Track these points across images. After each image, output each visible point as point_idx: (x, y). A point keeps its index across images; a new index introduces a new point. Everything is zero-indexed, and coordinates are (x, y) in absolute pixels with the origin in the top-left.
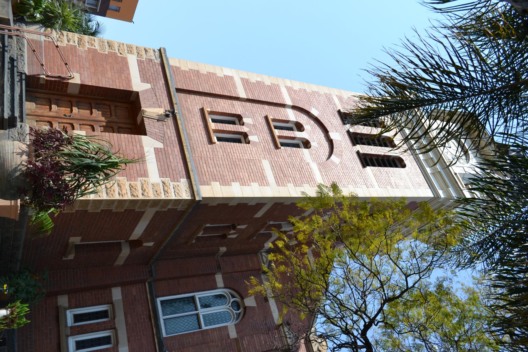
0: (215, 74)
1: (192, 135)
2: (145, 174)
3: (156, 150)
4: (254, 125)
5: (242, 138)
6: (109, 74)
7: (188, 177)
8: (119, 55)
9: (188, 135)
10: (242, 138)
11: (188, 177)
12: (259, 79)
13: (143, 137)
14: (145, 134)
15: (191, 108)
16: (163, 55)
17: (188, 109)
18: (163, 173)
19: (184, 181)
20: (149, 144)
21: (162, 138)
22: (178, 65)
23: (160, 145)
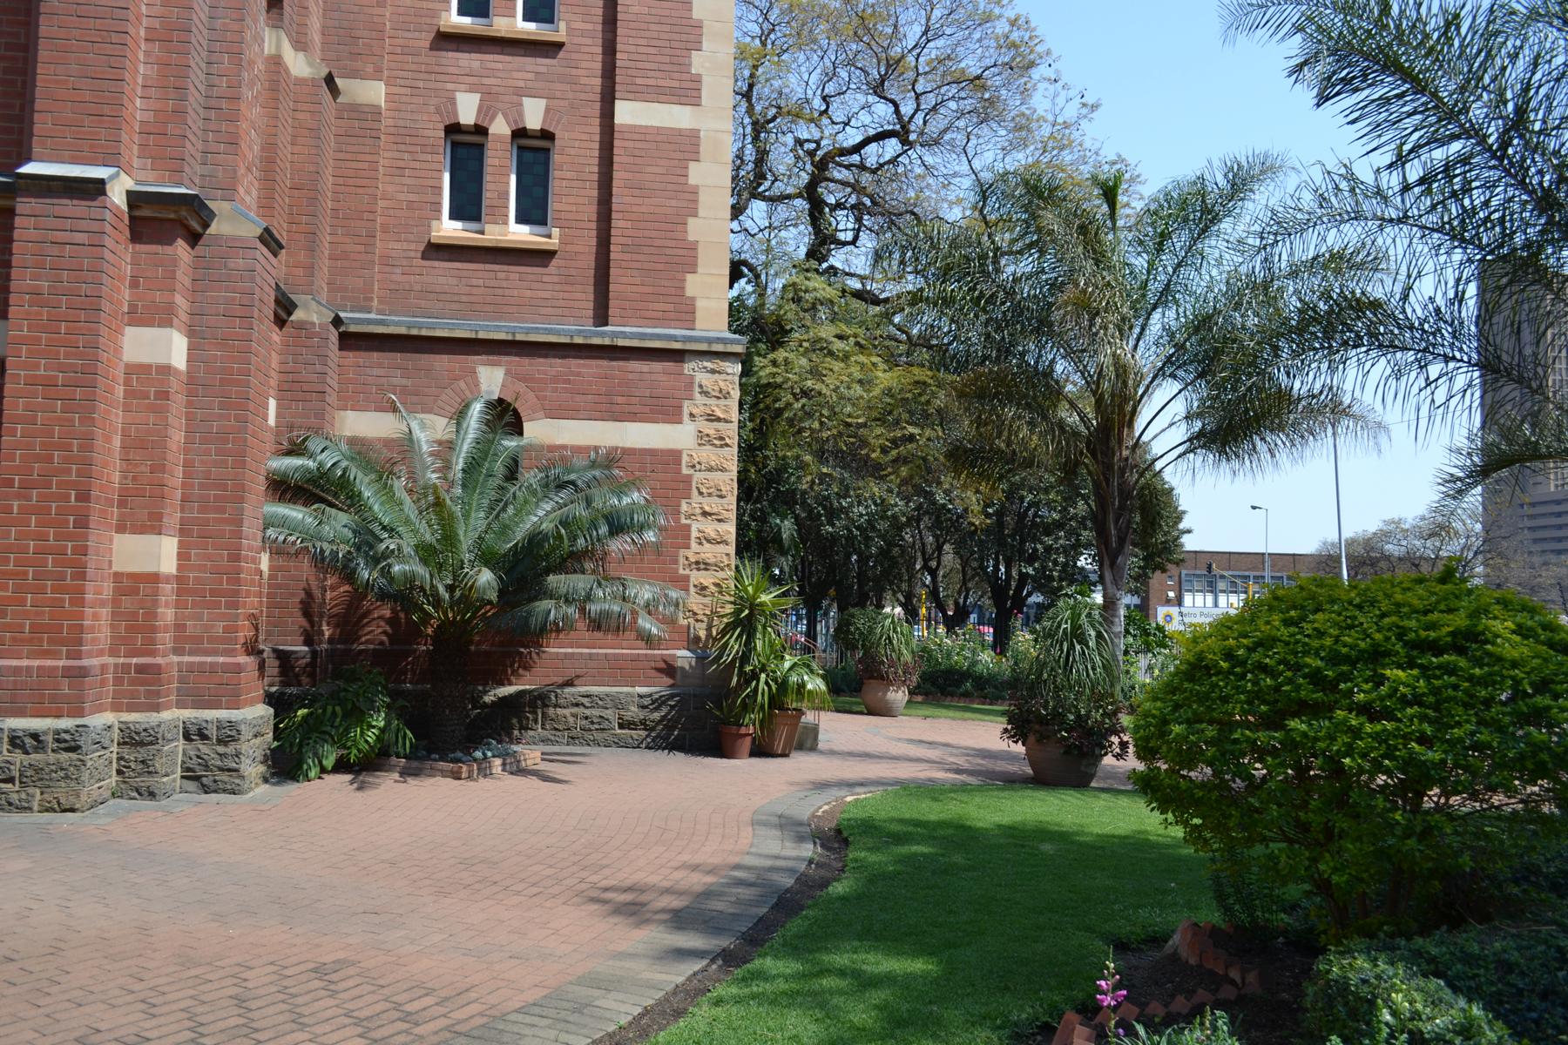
2: (674, 456)
5: (534, 150)
7: (678, 356)
10: (534, 150)
11: (678, 356)
18: (671, 414)
19: (689, 367)
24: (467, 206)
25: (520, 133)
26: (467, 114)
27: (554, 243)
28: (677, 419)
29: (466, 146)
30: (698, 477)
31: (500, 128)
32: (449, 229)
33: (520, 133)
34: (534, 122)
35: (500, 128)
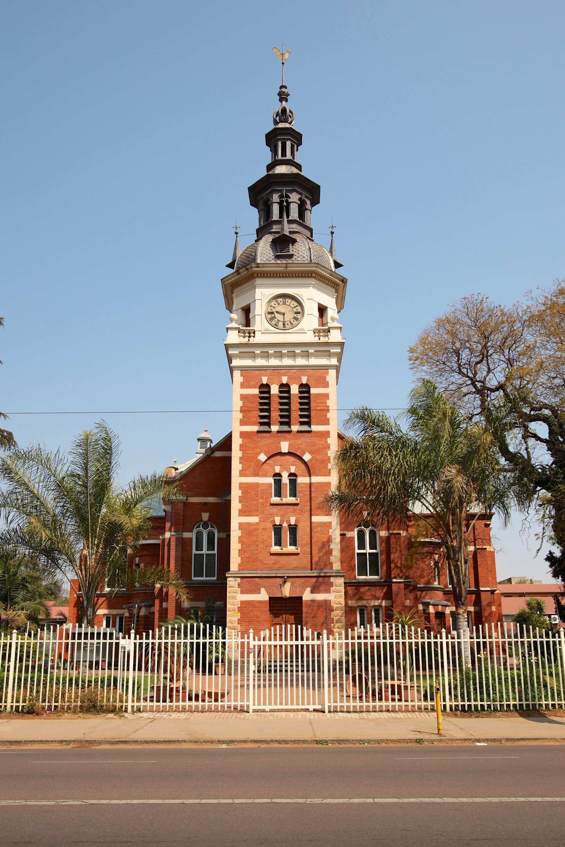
0: (240, 537)
1: (295, 566)
3: (312, 592)
4: (281, 516)
5: (293, 529)
6: (259, 614)
8: (239, 606)
9: (296, 568)
10: (293, 529)
11: (330, 576)
12: (238, 500)
13: (303, 599)
14: (302, 597)
15: (272, 562)
16: (233, 575)
17: (274, 564)
18: (328, 591)
19: (332, 579)
20: (307, 596)
21: (304, 588)
22: (237, 565)
23: (308, 590)
24: (278, 542)
25: (290, 525)
26: (278, 523)
27: (298, 551)
28: (330, 593)
29: (278, 529)
30: (335, 606)
31: (285, 525)
32: (276, 549)
33: (290, 525)
34: (293, 521)
35: (285, 525)
